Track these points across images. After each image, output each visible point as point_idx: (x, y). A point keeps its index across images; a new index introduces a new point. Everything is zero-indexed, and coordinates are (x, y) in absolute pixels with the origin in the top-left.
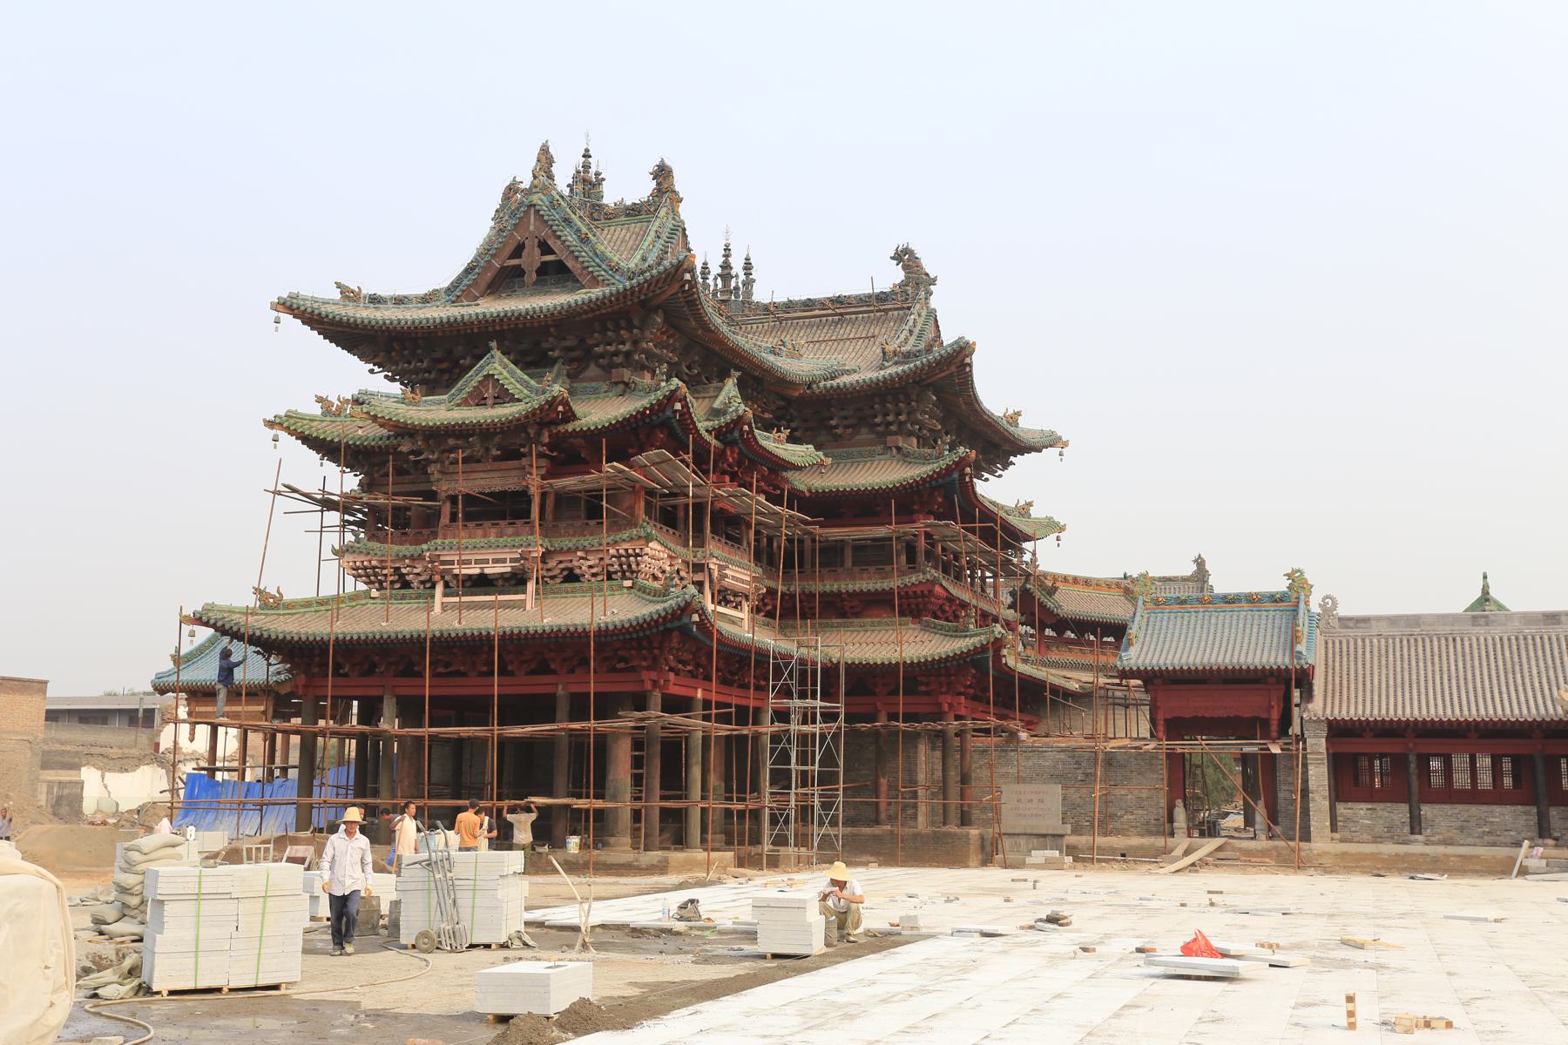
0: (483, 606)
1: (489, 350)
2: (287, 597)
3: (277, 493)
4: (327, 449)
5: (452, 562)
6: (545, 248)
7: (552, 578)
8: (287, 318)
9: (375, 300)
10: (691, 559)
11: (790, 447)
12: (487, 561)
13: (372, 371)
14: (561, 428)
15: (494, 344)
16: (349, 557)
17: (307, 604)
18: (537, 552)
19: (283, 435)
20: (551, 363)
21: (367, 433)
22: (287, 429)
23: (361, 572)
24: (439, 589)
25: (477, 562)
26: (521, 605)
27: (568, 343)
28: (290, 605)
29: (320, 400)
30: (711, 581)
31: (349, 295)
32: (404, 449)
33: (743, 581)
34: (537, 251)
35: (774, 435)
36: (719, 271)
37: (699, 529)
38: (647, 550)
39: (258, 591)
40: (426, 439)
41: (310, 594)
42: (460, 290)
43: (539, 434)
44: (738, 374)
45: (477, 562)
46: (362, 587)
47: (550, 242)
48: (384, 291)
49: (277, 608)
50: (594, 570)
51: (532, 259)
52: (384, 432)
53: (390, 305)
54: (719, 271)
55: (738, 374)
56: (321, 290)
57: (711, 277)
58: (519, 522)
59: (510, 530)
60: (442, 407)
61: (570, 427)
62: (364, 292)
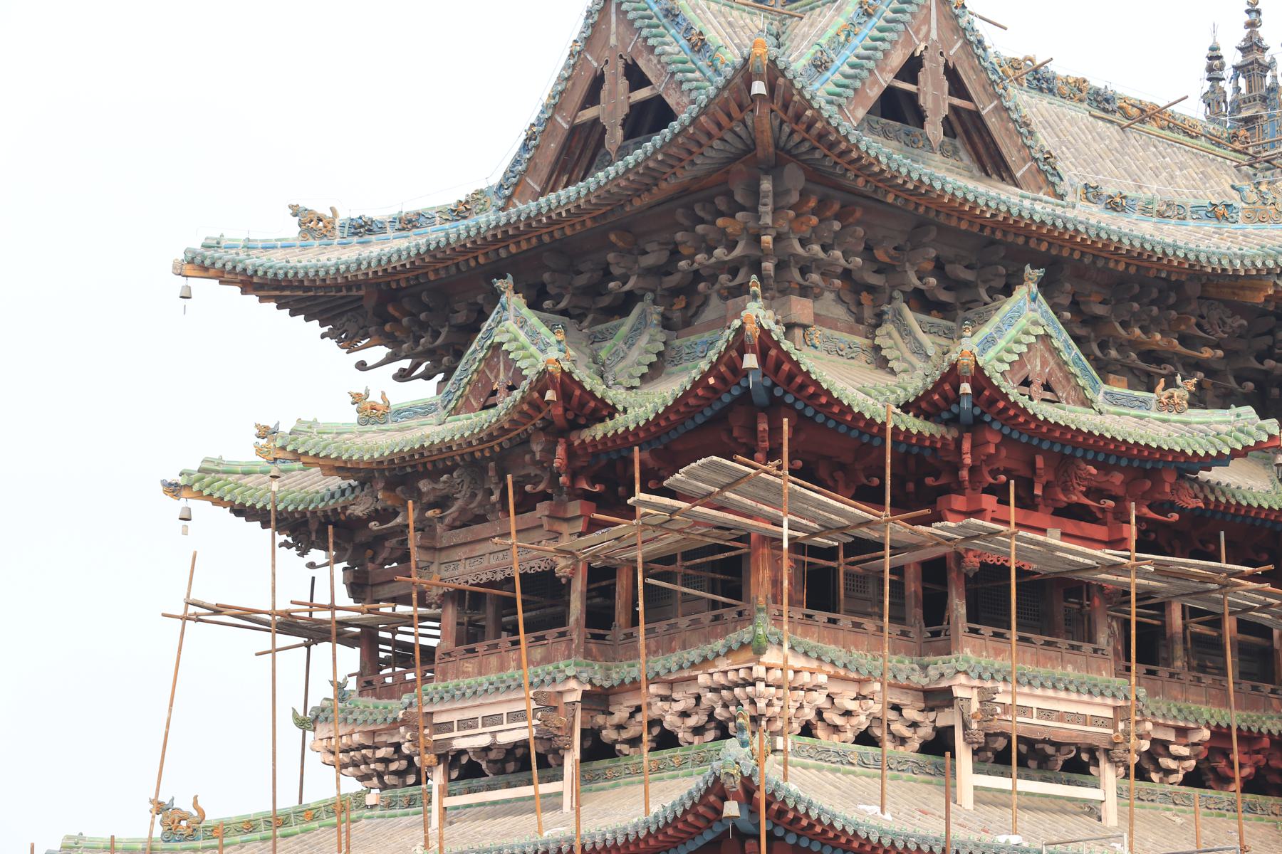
0: (1033, 804)
1: (495, 296)
2: (214, 814)
3: (185, 618)
4: (301, 528)
5: (447, 727)
6: (636, 77)
7: (635, 742)
8: (207, 288)
9: (363, 228)
10: (919, 680)
11: (1198, 416)
12: (496, 719)
13: (362, 366)
14: (587, 435)
15: (1033, 274)
16: (323, 730)
17: (249, 826)
18: (574, 692)
19: (201, 508)
20: (623, 306)
21: (314, 487)
22: (199, 495)
23: (350, 759)
24: (437, 779)
25: (487, 721)
26: (553, 802)
27: (648, 261)
28: (221, 831)
29: (265, 432)
30: (966, 727)
31: (314, 225)
32: (358, 511)
33: (1096, 720)
34: (623, 84)
35: (1161, 392)
36: (1238, 58)
37: (935, 613)
38: (759, 671)
39: (160, 808)
40: (390, 486)
41: (259, 805)
42: (513, 186)
43: (551, 451)
44: (1040, 272)
45: (487, 721)
46: (351, 785)
47: (641, 63)
48: (379, 211)
49: (191, 837)
50: (692, 721)
51: (618, 100)
52: (336, 482)
53: (390, 233)
54: (1238, 58)
55: (1040, 272)
56: (266, 229)
57: (1228, 72)
58: (551, 634)
59: (538, 653)
60: (432, 419)
61: (599, 431)
62: (343, 215)
